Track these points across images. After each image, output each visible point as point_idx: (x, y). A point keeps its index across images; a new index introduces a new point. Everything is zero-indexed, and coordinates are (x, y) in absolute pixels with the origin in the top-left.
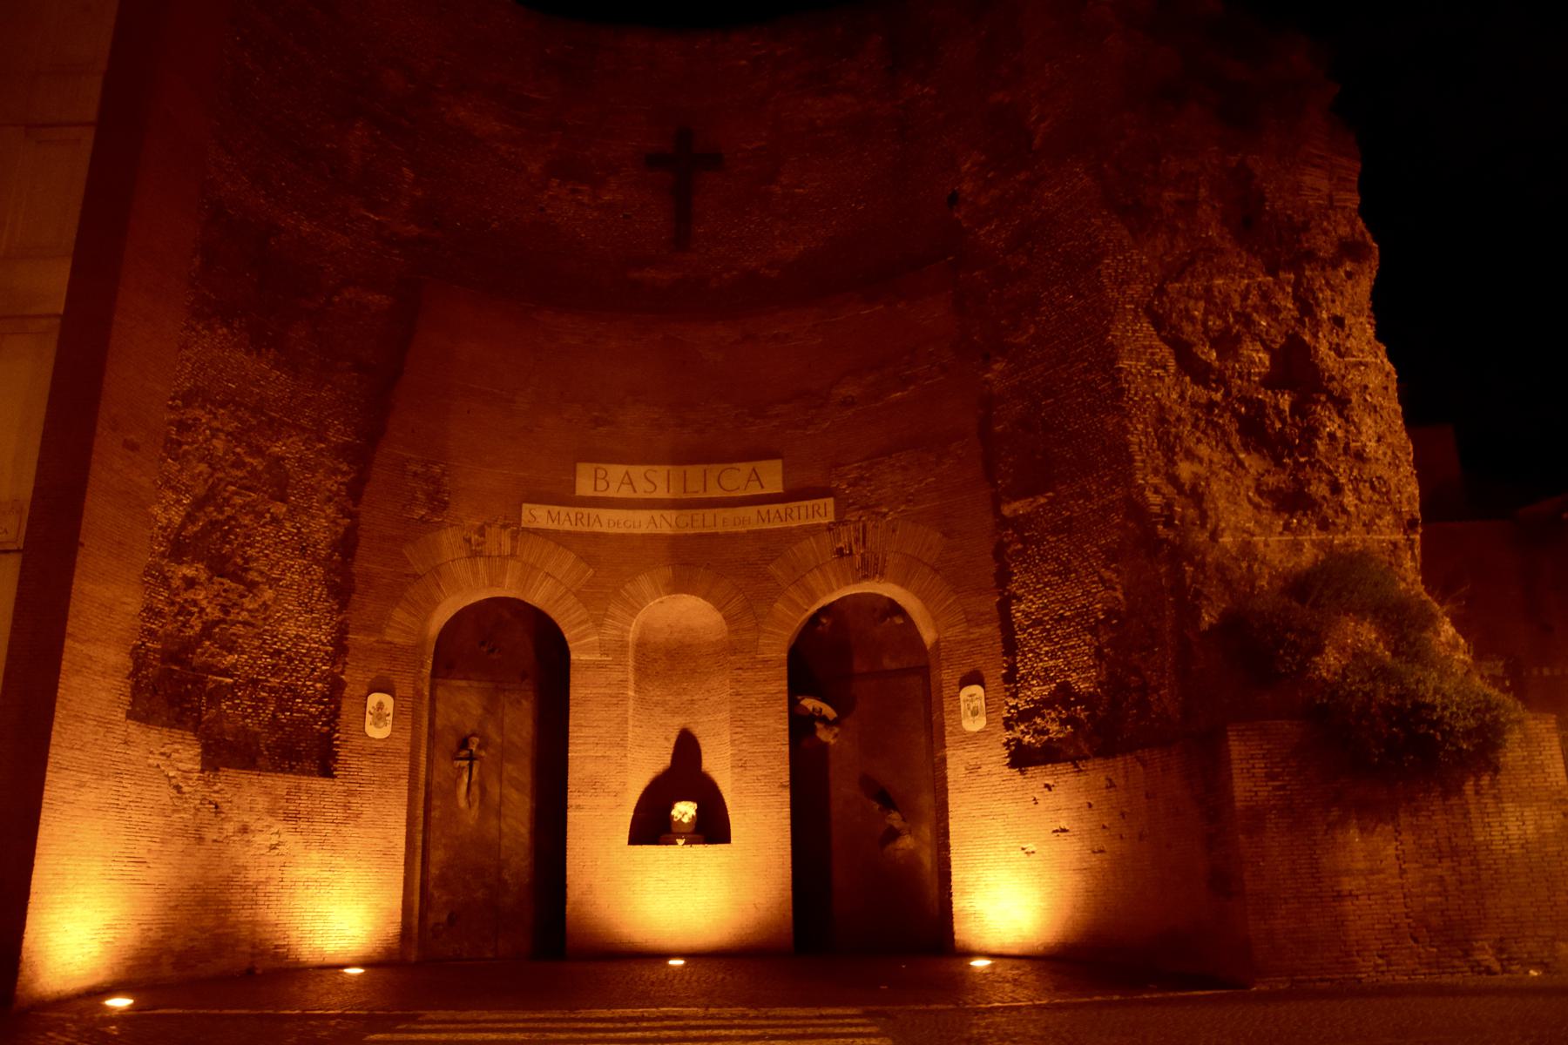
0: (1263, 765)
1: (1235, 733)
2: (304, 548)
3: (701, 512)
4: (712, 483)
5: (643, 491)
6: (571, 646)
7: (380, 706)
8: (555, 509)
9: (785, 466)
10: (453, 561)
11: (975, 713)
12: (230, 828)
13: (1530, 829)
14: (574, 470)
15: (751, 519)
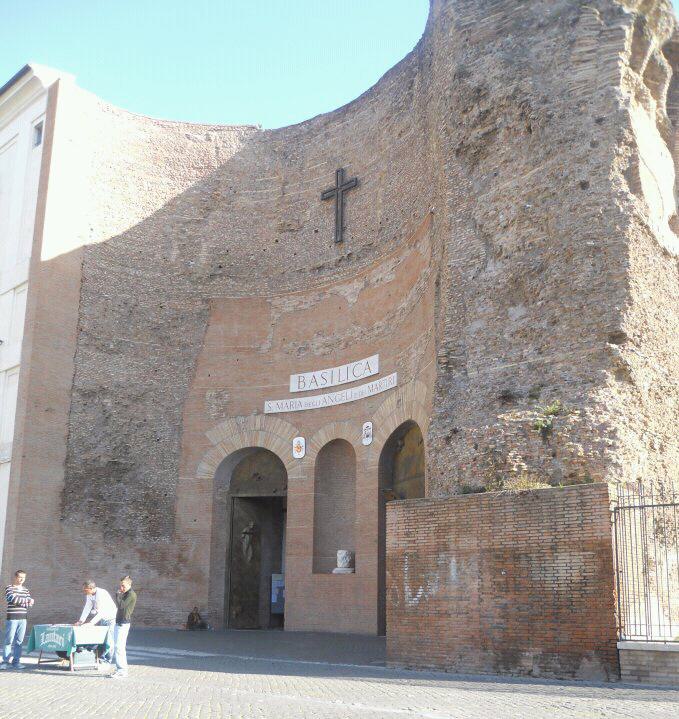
4: (350, 374)
15: (365, 391)
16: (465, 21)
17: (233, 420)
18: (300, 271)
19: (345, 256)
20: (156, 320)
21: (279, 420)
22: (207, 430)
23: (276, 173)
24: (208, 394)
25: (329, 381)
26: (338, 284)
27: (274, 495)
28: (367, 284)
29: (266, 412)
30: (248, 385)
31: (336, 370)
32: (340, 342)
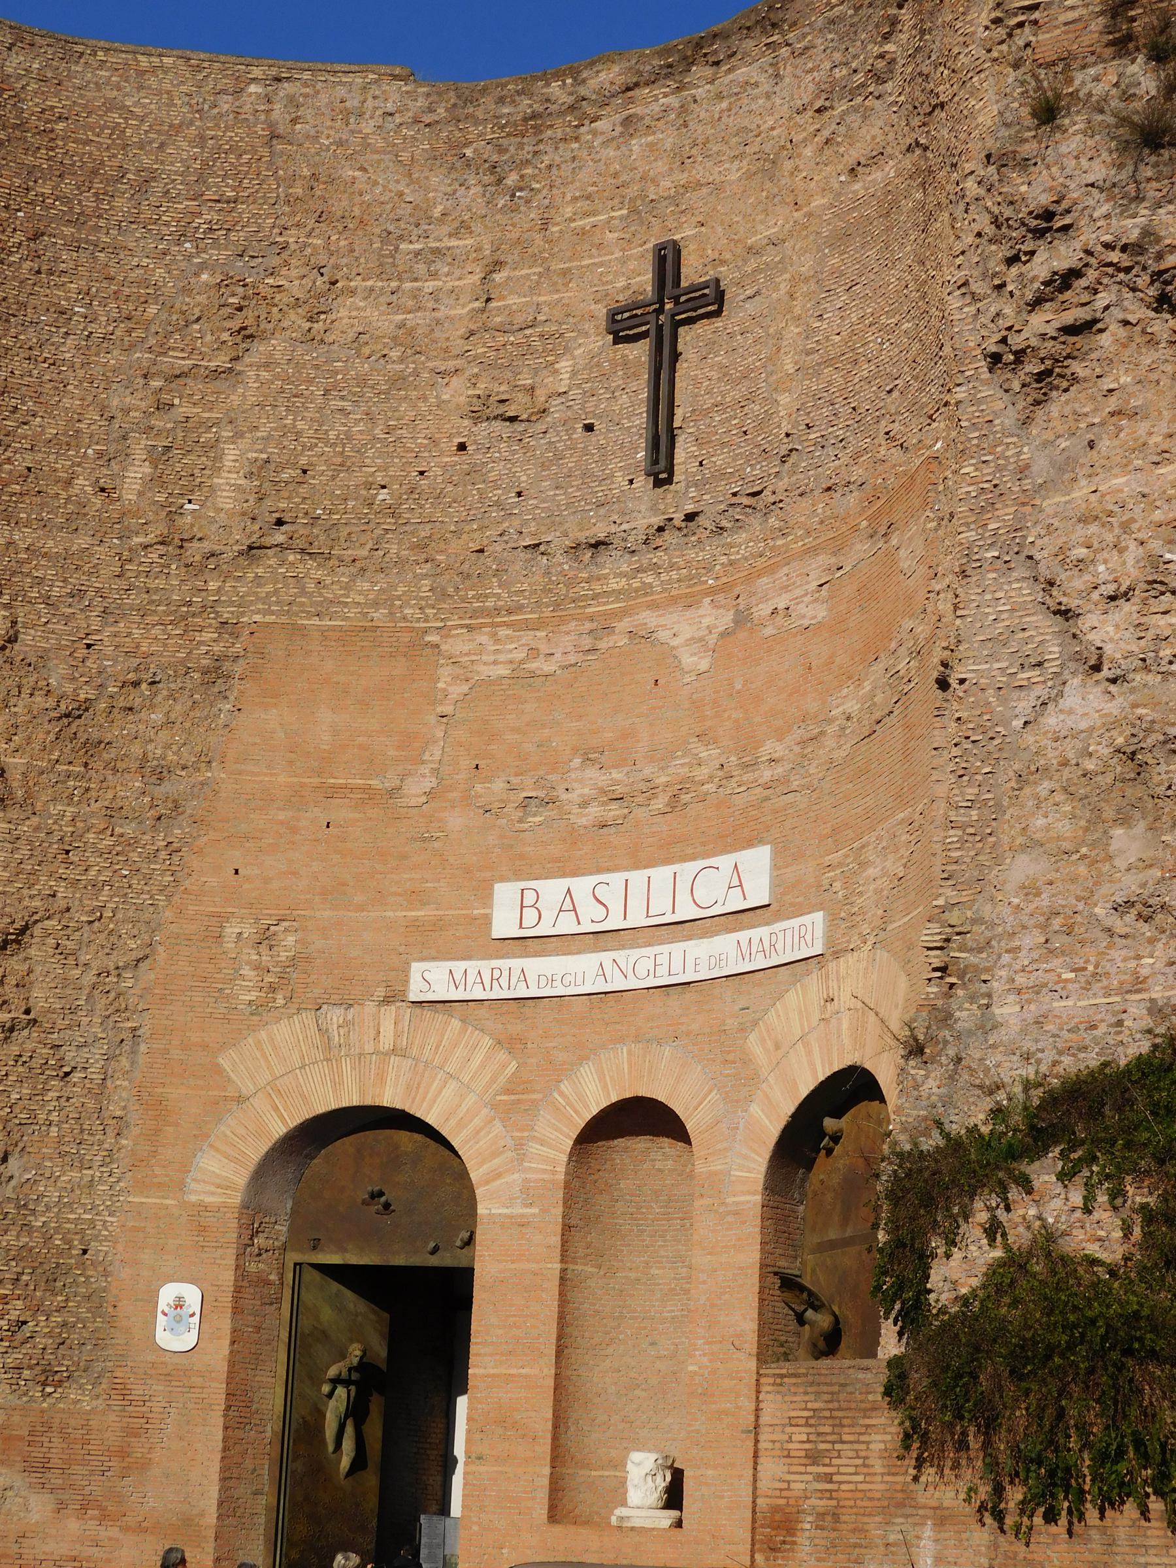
0: (804, 1438)
1: (771, 1380)
2: (67, 1074)
3: (665, 948)
4: (683, 896)
5: (590, 918)
6: (479, 1192)
7: (179, 1304)
8: (459, 966)
10: (303, 1067)
14: (490, 896)
17: (308, 1017)
19: (678, 517)
21: (456, 1023)
22: (223, 1046)
23: (462, 229)
24: (231, 931)
25: (616, 907)
26: (653, 606)
27: (434, 1261)
29: (413, 997)
30: (361, 908)
32: (651, 791)
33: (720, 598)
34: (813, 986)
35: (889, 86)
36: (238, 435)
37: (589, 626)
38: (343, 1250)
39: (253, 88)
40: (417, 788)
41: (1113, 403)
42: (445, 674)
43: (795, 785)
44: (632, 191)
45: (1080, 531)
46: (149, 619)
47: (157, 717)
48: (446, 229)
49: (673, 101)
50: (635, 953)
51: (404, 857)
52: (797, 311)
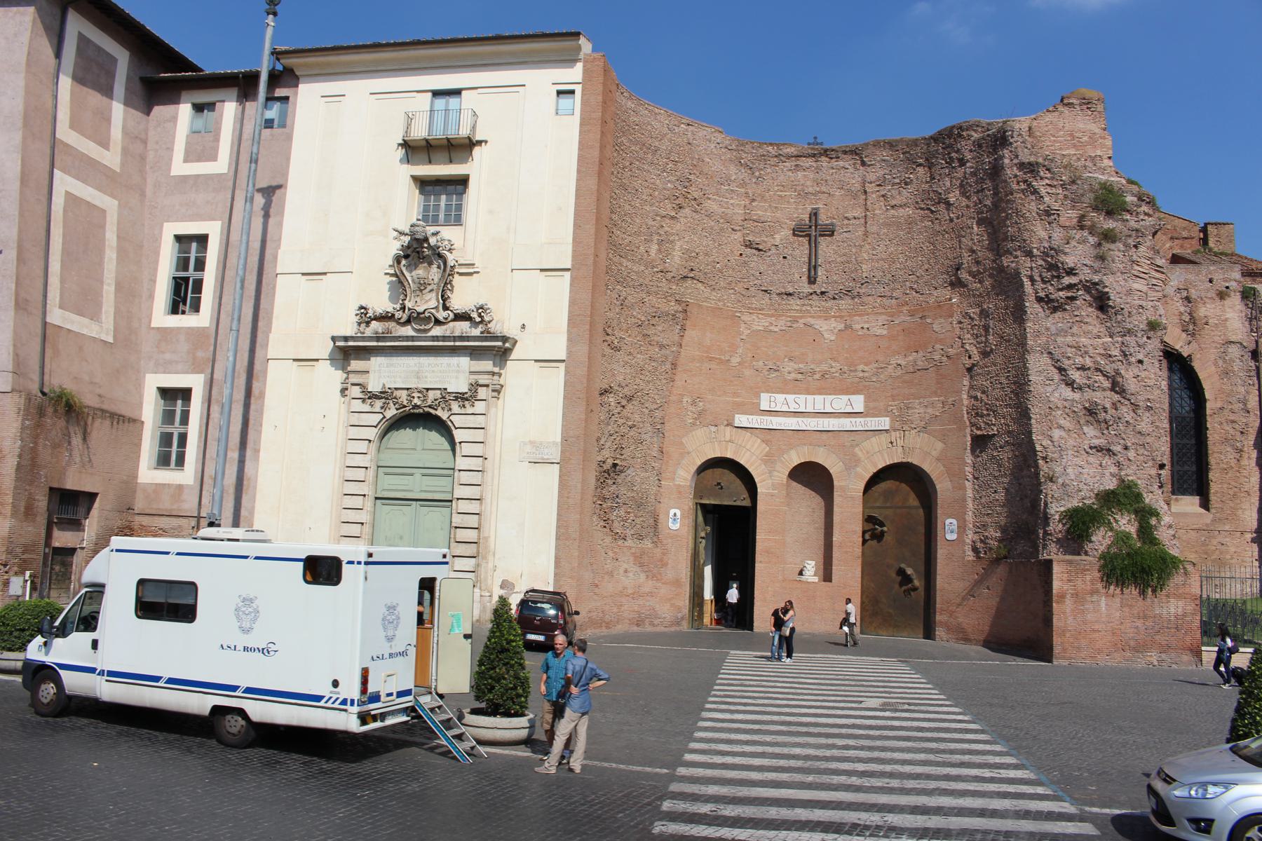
6: (758, 485)
7: (675, 515)
9: (865, 398)
11: (952, 532)
12: (621, 571)
13: (1180, 610)
15: (847, 424)
16: (1055, 206)
18: (766, 291)
19: (818, 291)
20: (639, 316)
24: (685, 400)
26: (813, 317)
27: (735, 504)
28: (848, 327)
31: (810, 398)
32: (814, 373)
33: (838, 319)
34: (884, 437)
35: (909, 187)
36: (680, 239)
37: (789, 319)
38: (709, 499)
39: (682, 126)
40: (735, 360)
41: (1078, 319)
42: (743, 325)
43: (874, 380)
44: (799, 188)
45: (1069, 349)
46: (659, 296)
47: (660, 328)
48: (735, 184)
49: (813, 164)
50: (810, 420)
51: (732, 381)
52: (869, 241)
